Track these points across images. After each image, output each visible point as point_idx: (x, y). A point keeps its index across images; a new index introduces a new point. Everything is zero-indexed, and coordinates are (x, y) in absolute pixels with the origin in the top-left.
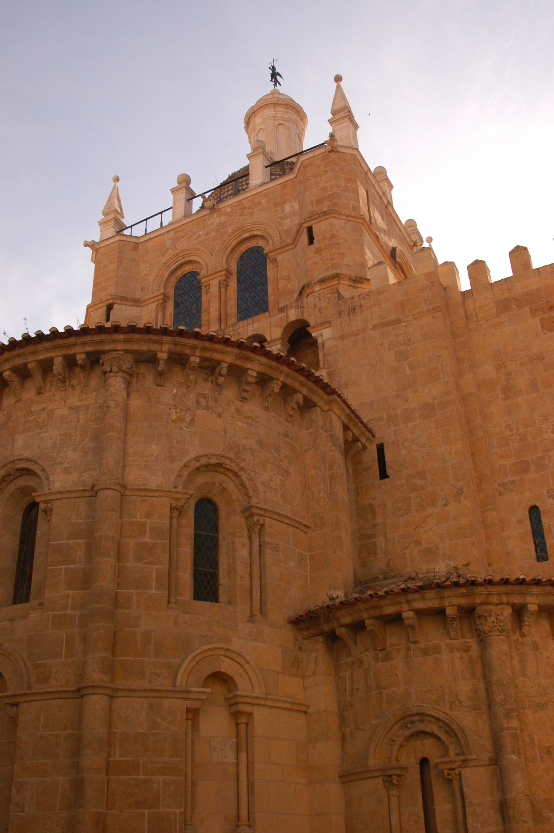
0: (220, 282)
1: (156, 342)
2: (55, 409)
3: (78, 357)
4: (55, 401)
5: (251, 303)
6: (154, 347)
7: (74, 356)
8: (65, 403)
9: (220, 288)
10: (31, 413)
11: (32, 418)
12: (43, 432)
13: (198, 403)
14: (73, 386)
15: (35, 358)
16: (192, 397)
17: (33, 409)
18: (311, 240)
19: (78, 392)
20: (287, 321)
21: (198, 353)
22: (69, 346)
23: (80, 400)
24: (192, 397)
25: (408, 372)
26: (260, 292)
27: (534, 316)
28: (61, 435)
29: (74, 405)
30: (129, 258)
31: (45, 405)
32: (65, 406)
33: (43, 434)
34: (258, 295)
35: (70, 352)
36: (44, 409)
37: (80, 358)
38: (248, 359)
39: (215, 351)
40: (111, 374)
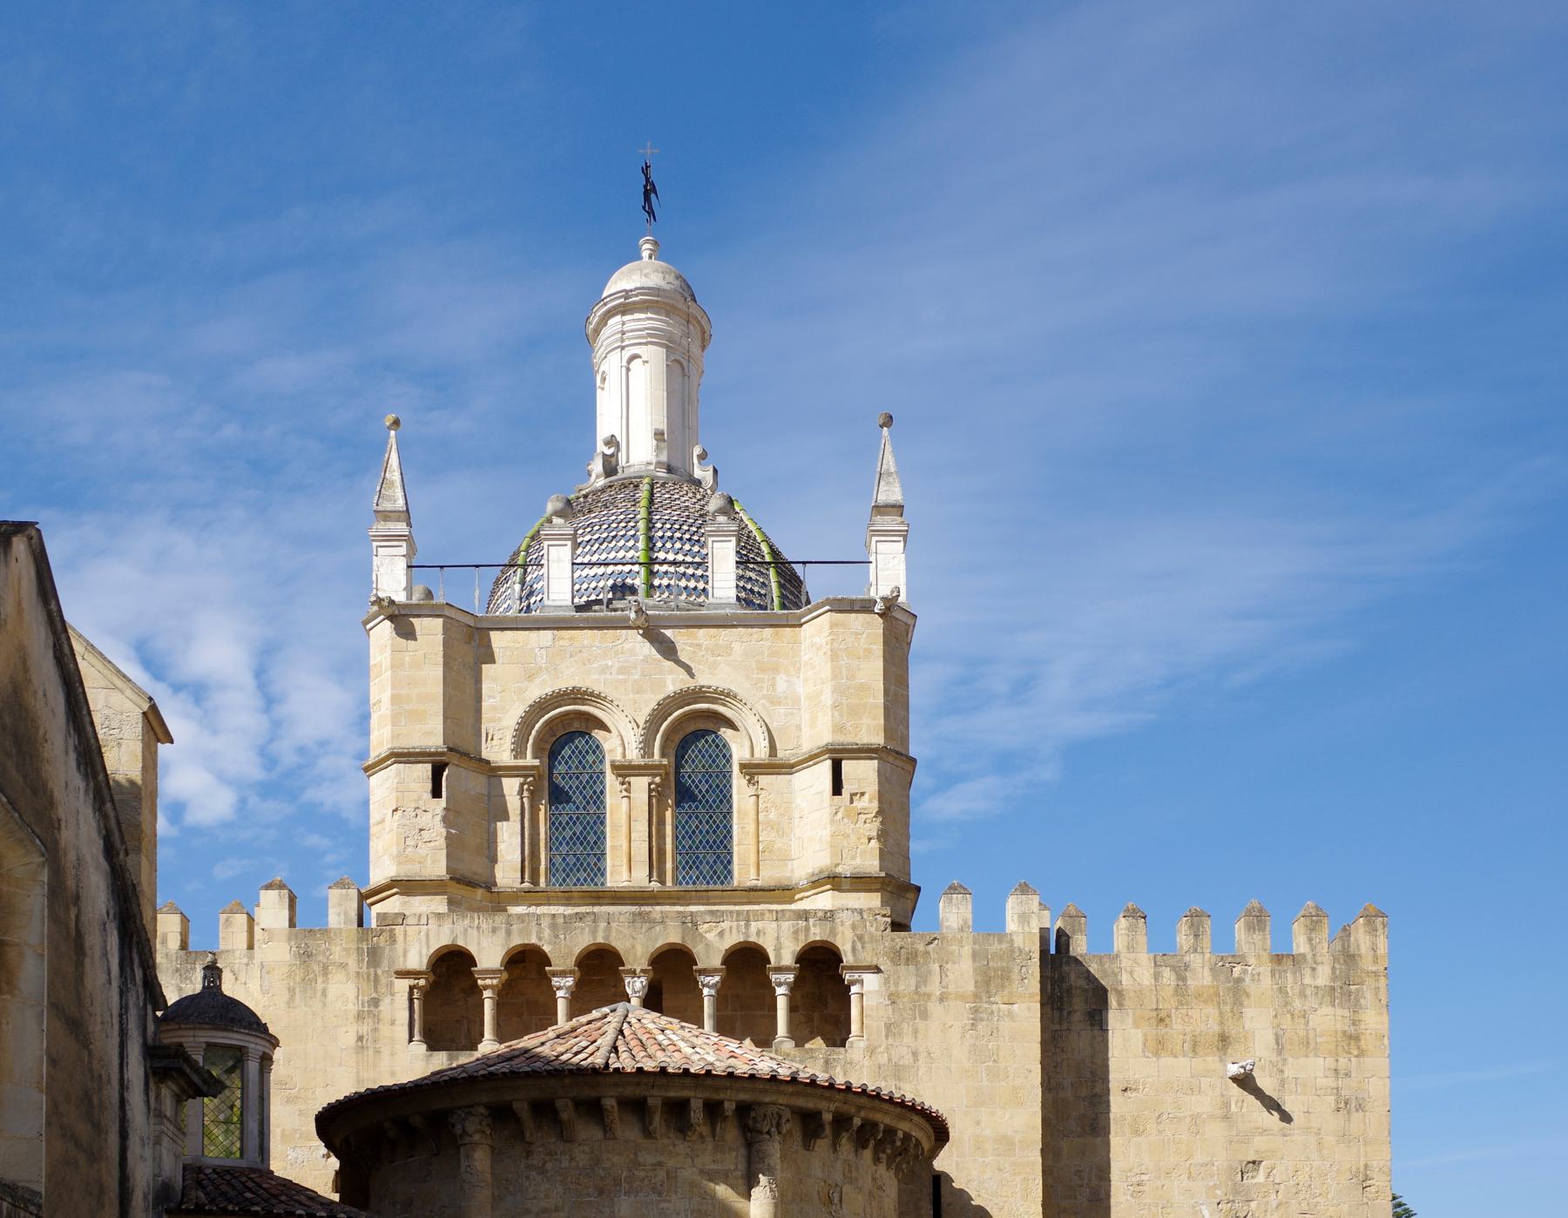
0: (650, 784)
1: (826, 1098)
2: (679, 1168)
3: (727, 1105)
4: (677, 1154)
5: (701, 842)
6: (822, 1105)
7: (720, 1103)
8: (693, 1161)
9: (650, 797)
10: (639, 1165)
11: (642, 1174)
12: (664, 1201)
13: (844, 1174)
14: (702, 1136)
15: (663, 1093)
16: (839, 1165)
17: (641, 1160)
18: (837, 789)
19: (710, 1147)
20: (806, 940)
21: (863, 1114)
22: (717, 1089)
23: (714, 1161)
24: (839, 1165)
25: (985, 1083)
26: (718, 827)
27: (1136, 1025)
28: (692, 1211)
29: (707, 1167)
30: (460, 660)
31: (662, 1159)
32: (694, 1166)
33: (663, 1205)
34: (715, 832)
35: (716, 1097)
36: (660, 1164)
37: (729, 1107)
38: (903, 1118)
39: (880, 1110)
40: (768, 1137)
